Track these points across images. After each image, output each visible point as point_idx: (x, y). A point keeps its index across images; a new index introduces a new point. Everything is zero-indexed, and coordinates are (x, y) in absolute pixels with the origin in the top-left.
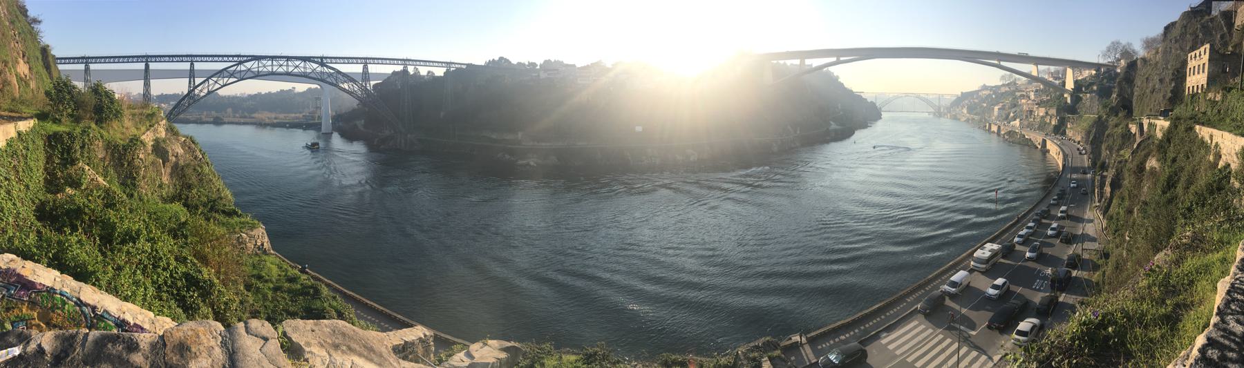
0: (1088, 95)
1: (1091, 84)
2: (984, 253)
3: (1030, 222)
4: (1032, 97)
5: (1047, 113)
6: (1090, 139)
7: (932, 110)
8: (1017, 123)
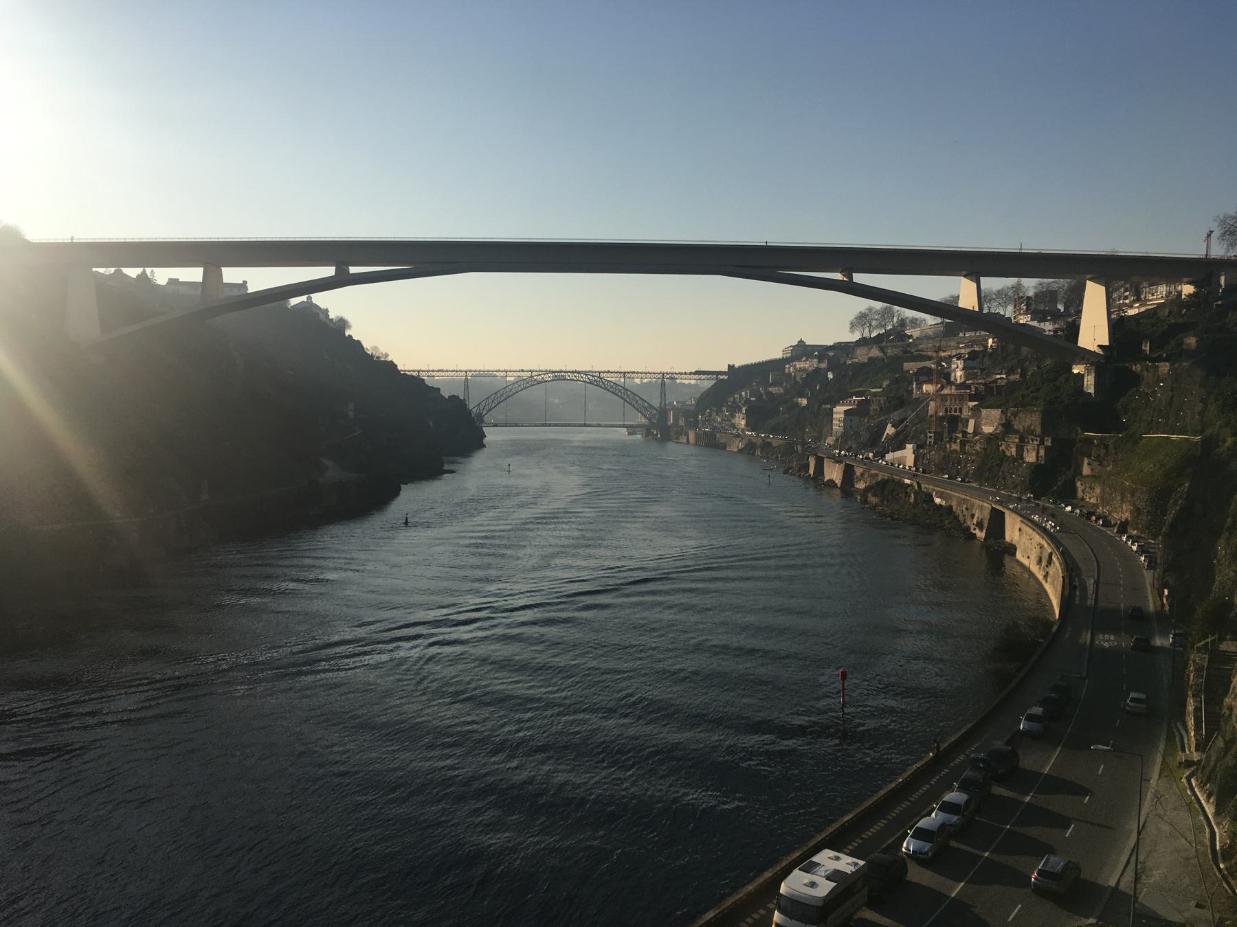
0: (1164, 367)
1: (1177, 330)
2: (813, 885)
3: (950, 788)
4: (959, 375)
5: (1007, 427)
6: (1169, 518)
7: (641, 420)
8: (907, 455)
